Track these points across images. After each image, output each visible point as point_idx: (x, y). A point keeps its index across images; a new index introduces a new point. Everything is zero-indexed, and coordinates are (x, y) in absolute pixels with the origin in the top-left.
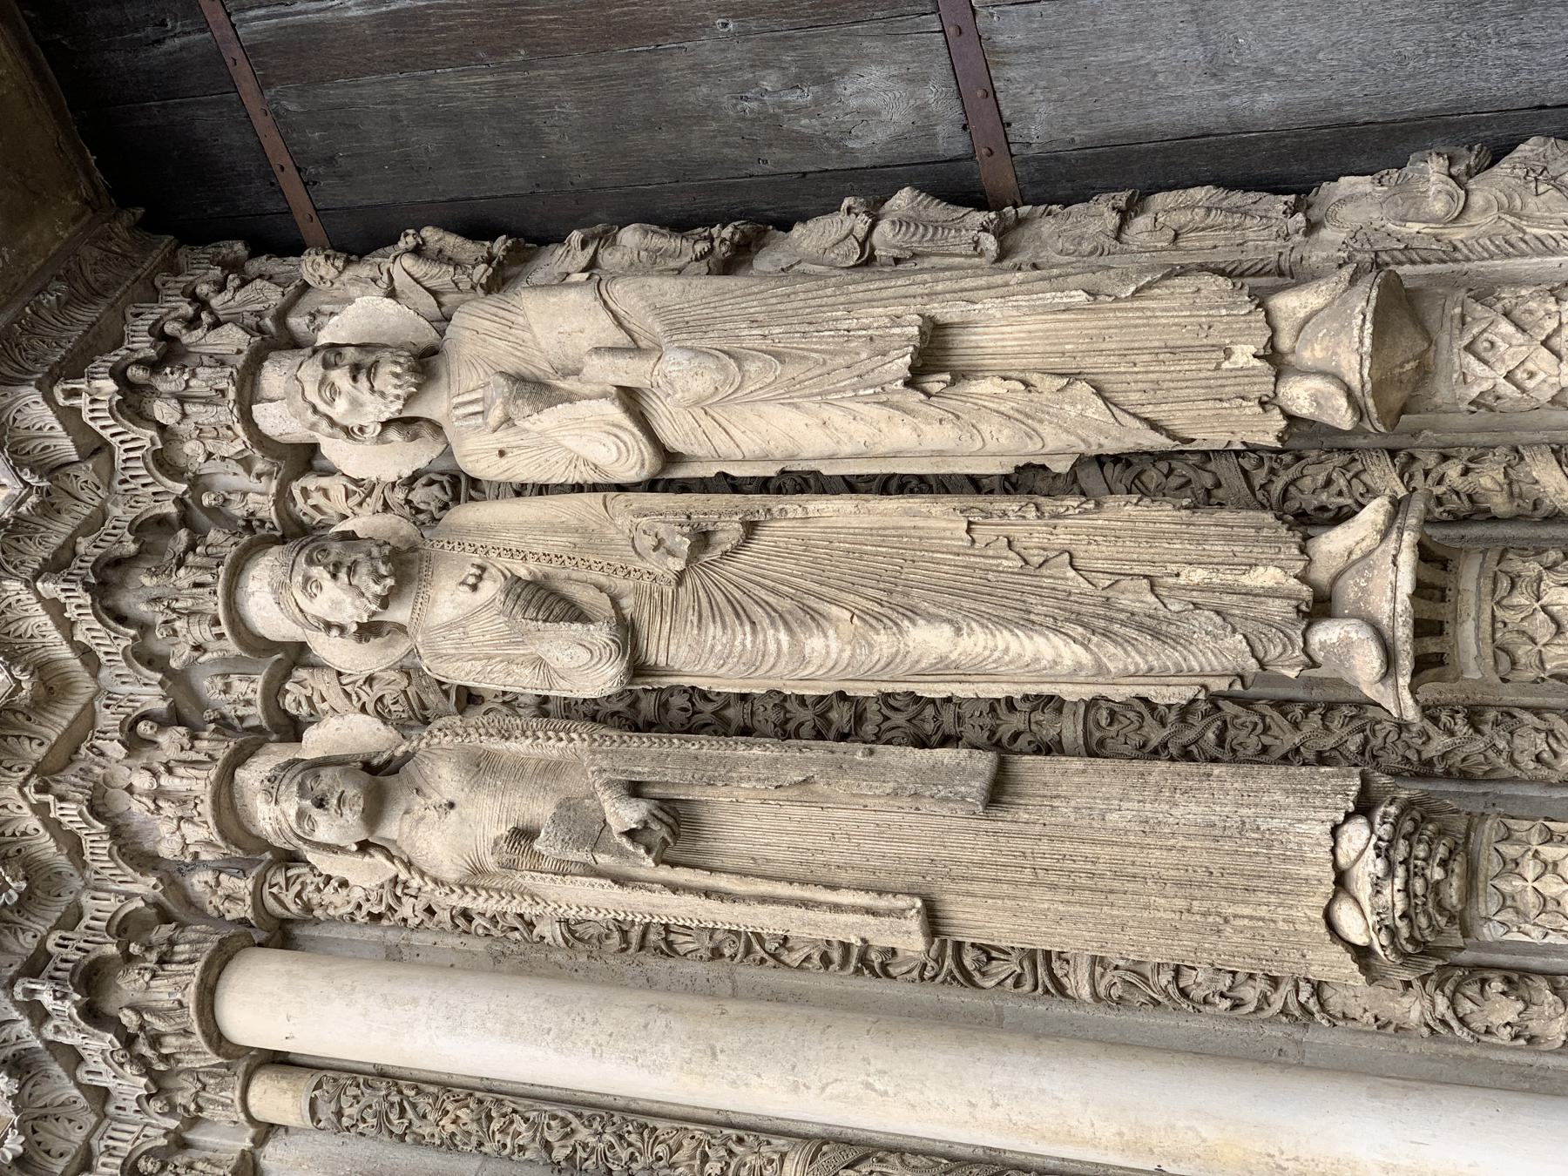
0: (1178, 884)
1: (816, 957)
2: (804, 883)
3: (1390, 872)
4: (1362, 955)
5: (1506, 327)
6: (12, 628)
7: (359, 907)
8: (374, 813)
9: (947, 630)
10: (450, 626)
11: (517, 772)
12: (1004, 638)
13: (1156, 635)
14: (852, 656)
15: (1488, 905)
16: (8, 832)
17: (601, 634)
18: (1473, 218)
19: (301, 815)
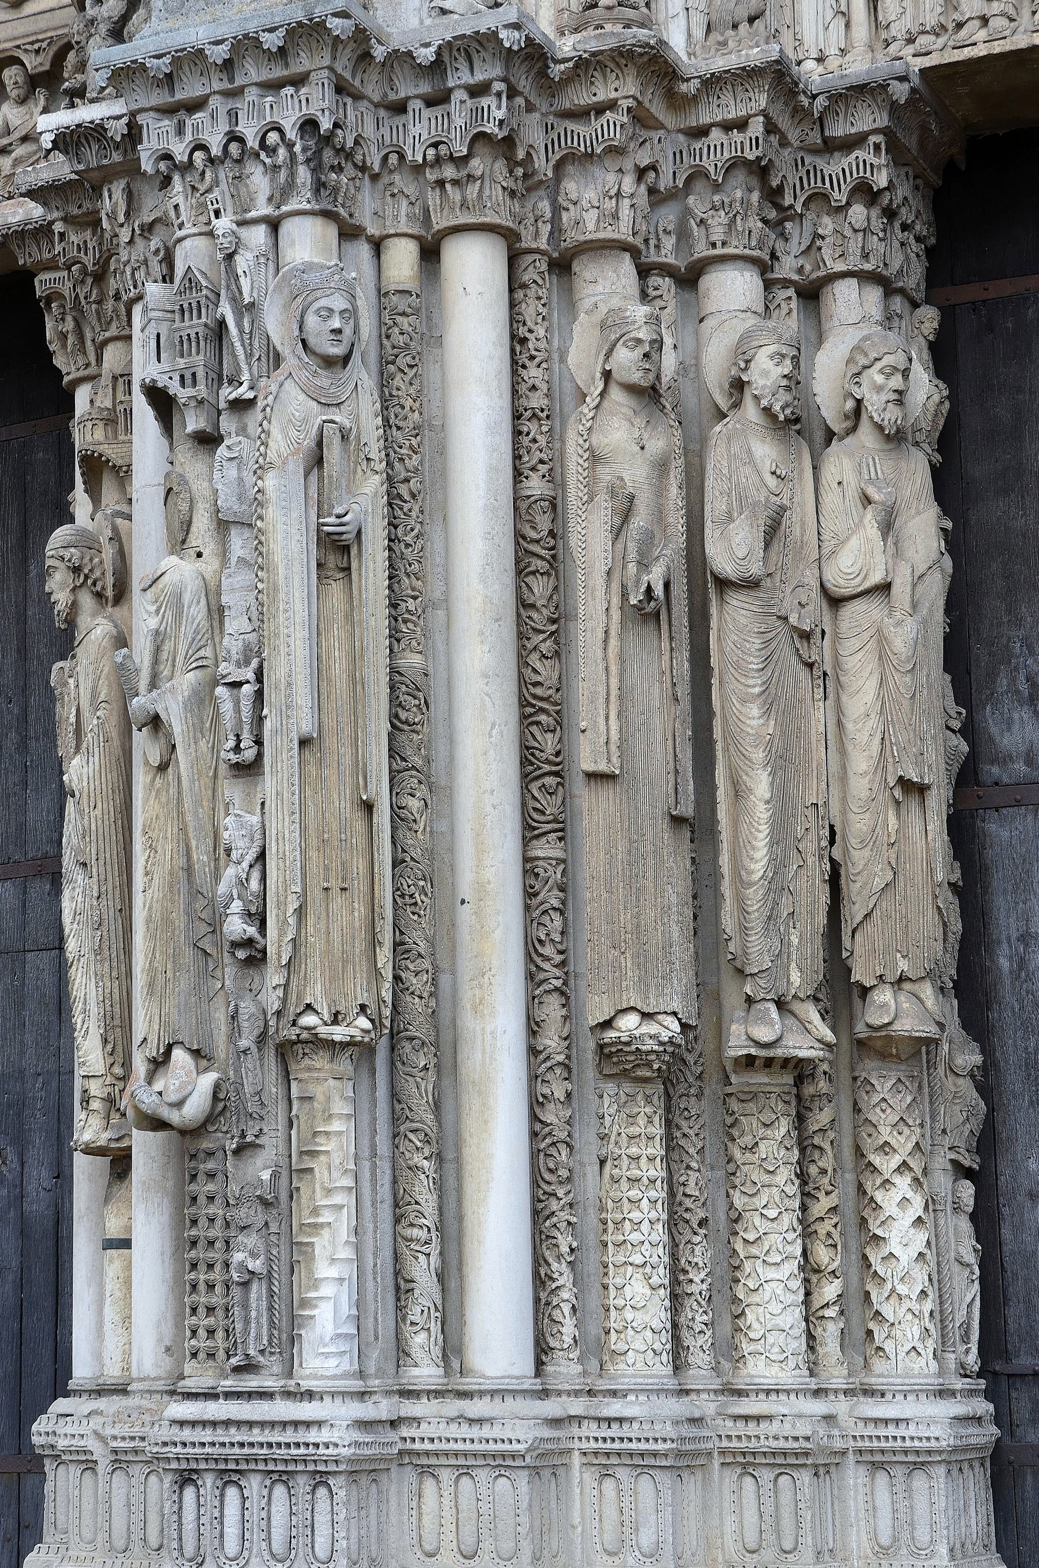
0: (638, 926)
1: (539, 679)
2: (620, 698)
3: (661, 1044)
4: (607, 1024)
5: (909, 1099)
6: (729, 87)
7: (530, 331)
8: (632, 389)
9: (768, 796)
10: (749, 452)
11: (660, 491)
12: (765, 829)
13: (769, 918)
14: (748, 734)
15: (628, 1087)
16: (596, 74)
17: (755, 569)
18: (951, 1078)
19: (639, 341)
